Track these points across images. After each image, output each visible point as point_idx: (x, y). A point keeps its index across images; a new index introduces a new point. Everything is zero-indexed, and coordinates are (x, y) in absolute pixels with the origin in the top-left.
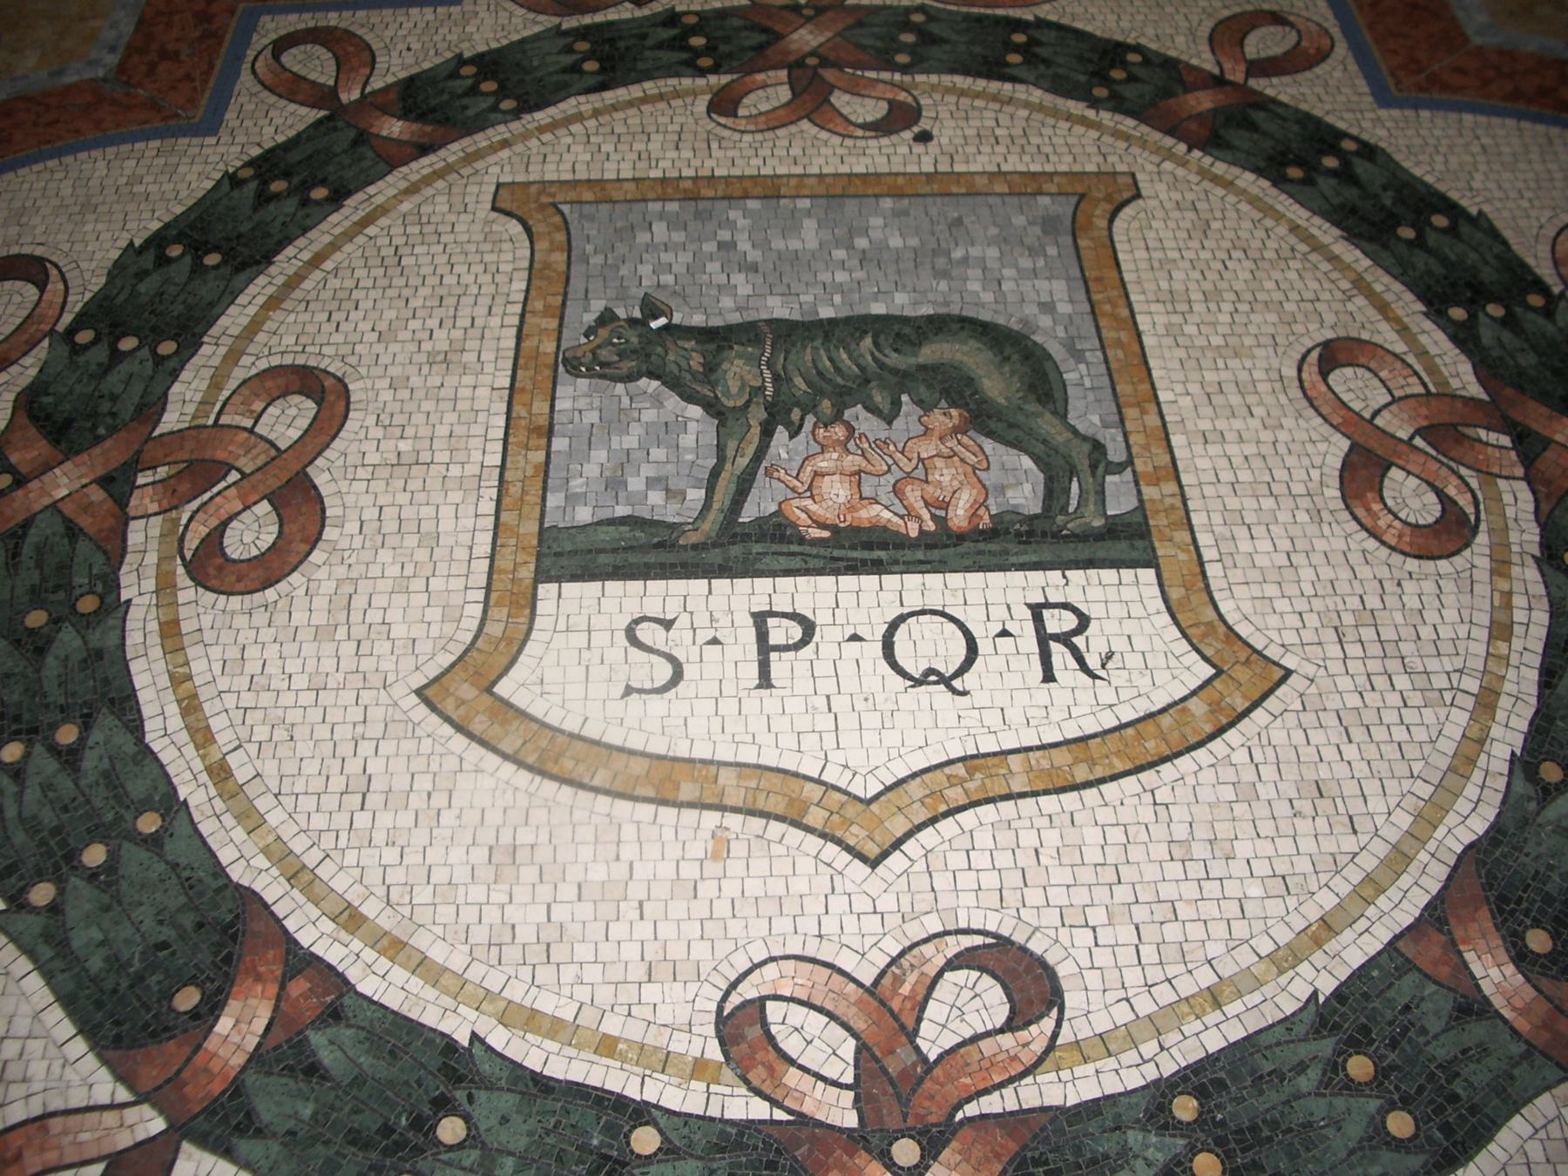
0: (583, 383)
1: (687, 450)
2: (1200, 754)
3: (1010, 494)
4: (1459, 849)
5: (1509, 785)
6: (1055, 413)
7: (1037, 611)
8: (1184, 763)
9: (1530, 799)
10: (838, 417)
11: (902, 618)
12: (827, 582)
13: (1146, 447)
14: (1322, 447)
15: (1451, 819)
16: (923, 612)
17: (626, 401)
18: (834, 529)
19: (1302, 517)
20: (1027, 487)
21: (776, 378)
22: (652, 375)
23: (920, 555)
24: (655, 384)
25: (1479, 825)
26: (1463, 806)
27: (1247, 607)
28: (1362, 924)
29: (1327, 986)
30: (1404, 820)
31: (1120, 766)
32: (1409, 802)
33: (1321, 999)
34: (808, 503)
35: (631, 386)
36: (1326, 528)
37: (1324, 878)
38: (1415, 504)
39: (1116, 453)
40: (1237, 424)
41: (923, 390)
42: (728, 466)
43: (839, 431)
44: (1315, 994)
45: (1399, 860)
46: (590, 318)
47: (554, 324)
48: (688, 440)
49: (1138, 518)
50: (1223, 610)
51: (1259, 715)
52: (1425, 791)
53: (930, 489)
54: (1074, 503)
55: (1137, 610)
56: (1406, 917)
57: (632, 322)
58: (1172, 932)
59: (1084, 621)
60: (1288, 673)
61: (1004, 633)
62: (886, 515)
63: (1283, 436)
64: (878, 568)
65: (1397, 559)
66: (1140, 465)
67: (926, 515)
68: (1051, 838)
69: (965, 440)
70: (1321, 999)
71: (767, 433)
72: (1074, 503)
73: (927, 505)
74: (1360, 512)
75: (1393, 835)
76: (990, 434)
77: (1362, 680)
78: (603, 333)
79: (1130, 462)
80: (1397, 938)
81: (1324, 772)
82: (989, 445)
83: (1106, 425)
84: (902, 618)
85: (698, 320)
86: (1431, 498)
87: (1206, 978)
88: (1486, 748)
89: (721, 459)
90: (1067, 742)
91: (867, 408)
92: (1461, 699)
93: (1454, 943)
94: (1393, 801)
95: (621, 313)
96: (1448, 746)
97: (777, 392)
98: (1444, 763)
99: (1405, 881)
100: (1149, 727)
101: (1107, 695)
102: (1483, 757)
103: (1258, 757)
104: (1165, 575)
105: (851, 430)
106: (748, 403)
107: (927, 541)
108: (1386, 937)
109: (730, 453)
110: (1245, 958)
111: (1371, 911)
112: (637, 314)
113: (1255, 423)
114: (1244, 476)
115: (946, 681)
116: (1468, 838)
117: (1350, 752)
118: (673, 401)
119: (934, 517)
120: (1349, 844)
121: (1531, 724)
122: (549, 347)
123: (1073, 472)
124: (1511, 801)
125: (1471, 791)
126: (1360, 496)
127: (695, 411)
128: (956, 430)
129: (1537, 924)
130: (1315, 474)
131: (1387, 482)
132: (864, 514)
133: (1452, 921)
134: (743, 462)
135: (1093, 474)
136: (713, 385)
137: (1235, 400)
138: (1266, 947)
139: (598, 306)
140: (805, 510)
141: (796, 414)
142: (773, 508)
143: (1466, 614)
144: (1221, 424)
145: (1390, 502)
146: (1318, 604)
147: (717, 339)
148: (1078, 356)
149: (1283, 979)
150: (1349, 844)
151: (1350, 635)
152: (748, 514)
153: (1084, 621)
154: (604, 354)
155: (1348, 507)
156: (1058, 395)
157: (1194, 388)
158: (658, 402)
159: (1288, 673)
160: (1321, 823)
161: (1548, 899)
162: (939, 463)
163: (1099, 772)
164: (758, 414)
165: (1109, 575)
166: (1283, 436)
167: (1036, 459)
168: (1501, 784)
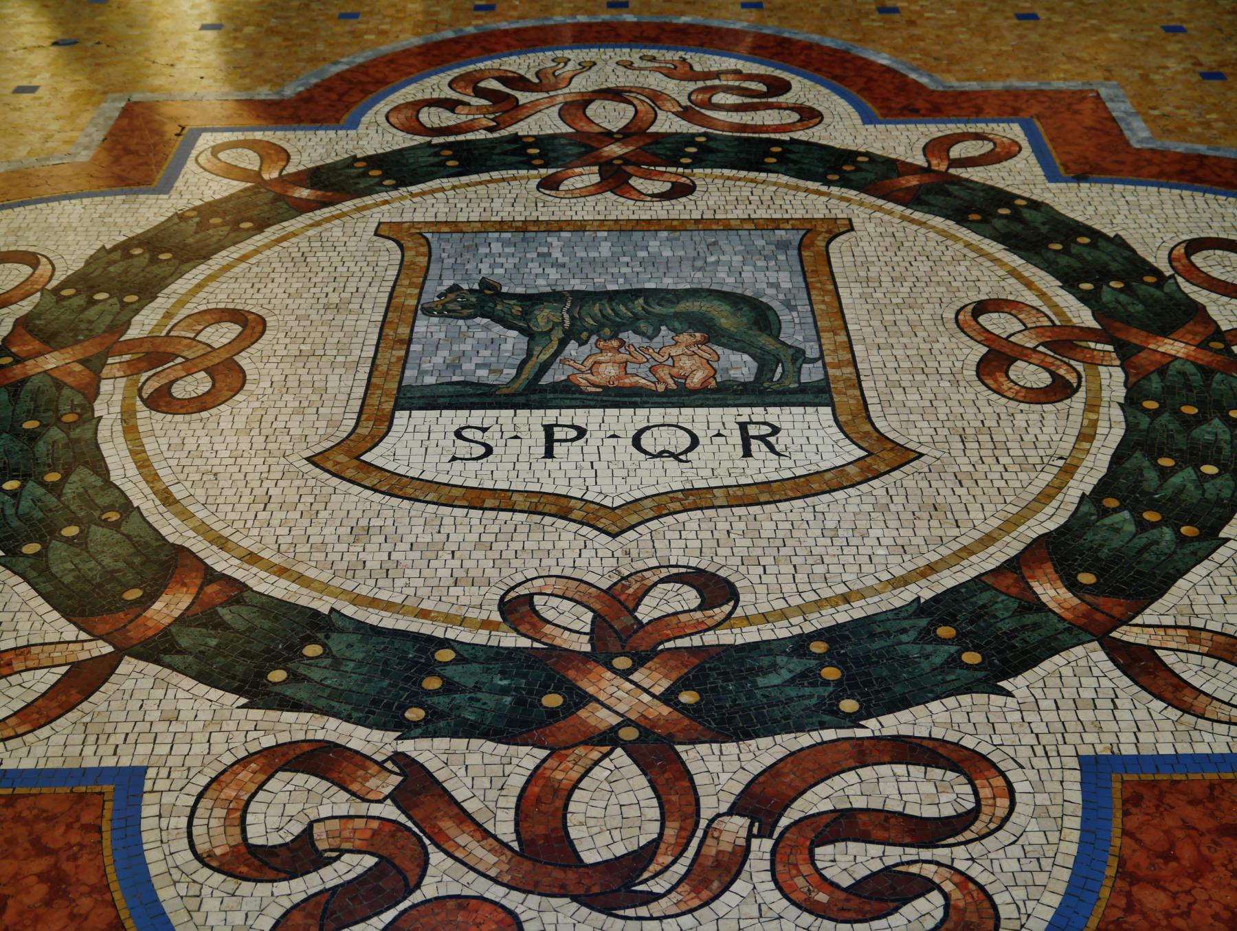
0: (435, 320)
1: (506, 351)
2: (851, 491)
3: (732, 372)
4: (1035, 536)
5: (1077, 509)
6: (770, 335)
7: (743, 427)
8: (839, 495)
9: (1092, 514)
10: (615, 336)
11: (648, 428)
12: (599, 411)
13: (835, 351)
14: (967, 351)
15: (1031, 522)
16: (663, 425)
17: (464, 329)
18: (606, 388)
19: (945, 384)
20: (745, 370)
21: (572, 318)
22: (483, 316)
23: (665, 400)
24: (486, 321)
25: (1052, 526)
26: (1041, 517)
27: (896, 425)
28: (958, 568)
29: (927, 595)
30: (996, 523)
31: (791, 494)
32: (1002, 515)
33: (922, 601)
34: (590, 377)
35: (469, 322)
36: (962, 390)
37: (931, 547)
38: (1034, 378)
39: (812, 351)
40: (903, 340)
41: (677, 325)
42: (534, 359)
43: (615, 343)
44: (919, 598)
45: (988, 540)
46: (442, 289)
47: (417, 291)
48: (507, 347)
49: (824, 383)
50: (877, 425)
51: (897, 474)
52: (1015, 510)
53: (676, 370)
54: (777, 376)
55: (815, 425)
56: (989, 566)
57: (471, 291)
58: (820, 569)
59: (775, 430)
60: (921, 455)
61: (719, 435)
62: (643, 381)
63: (936, 346)
64: (635, 406)
65: (1013, 404)
66: (828, 359)
67: (670, 381)
68: (742, 526)
69: (704, 347)
70: (922, 601)
71: (563, 343)
72: (777, 376)
73: (672, 377)
74: (990, 382)
75: (987, 529)
76: (724, 345)
77: (975, 459)
78: (451, 296)
79: (822, 357)
80: (981, 575)
81: (940, 500)
82: (720, 350)
83: (806, 340)
84: (648, 428)
85: (520, 290)
86: (1047, 375)
87: (842, 589)
88: (1064, 490)
89: (530, 353)
90: (755, 484)
91: (635, 332)
92: (1048, 468)
93: (1023, 578)
94: (988, 514)
95: (465, 287)
96: (1035, 490)
97: (572, 325)
98: (1031, 498)
99: (991, 550)
100: (816, 477)
101: (786, 463)
102: (1060, 497)
103: (892, 492)
104: (838, 411)
105: (623, 343)
106: (551, 330)
107: (668, 393)
108: (974, 574)
109: (536, 353)
110: (870, 581)
111: (965, 563)
112: (476, 287)
113: (919, 340)
114: (905, 364)
115: (676, 456)
116: (1042, 531)
117: (959, 491)
118: (498, 329)
119: (675, 383)
120: (956, 532)
121: (1100, 480)
122: (414, 302)
123: (779, 361)
124: (1079, 514)
125: (1049, 510)
126: (991, 374)
127: (514, 333)
128: (697, 343)
129: (1087, 570)
130: (959, 364)
131: (1012, 368)
132: (627, 381)
133: (1024, 569)
134: (543, 357)
135: (793, 364)
136: (527, 321)
137: (905, 329)
138: (885, 576)
139: (448, 283)
140: (586, 379)
141: (584, 335)
142: (563, 378)
143: (1060, 430)
144: (892, 340)
145: (1012, 377)
146: (947, 424)
147: (532, 301)
148: (791, 307)
149: (896, 592)
150: (956, 532)
151: (971, 438)
152: (546, 379)
153: (775, 430)
154: (450, 306)
155: (980, 379)
156: (775, 327)
157: (876, 324)
158: (486, 328)
159: (921, 455)
160: (934, 523)
161: (1099, 560)
162: (684, 358)
163: (777, 498)
164: (558, 334)
165: (801, 410)
166: (936, 346)
167: (753, 357)
168: (1073, 508)
